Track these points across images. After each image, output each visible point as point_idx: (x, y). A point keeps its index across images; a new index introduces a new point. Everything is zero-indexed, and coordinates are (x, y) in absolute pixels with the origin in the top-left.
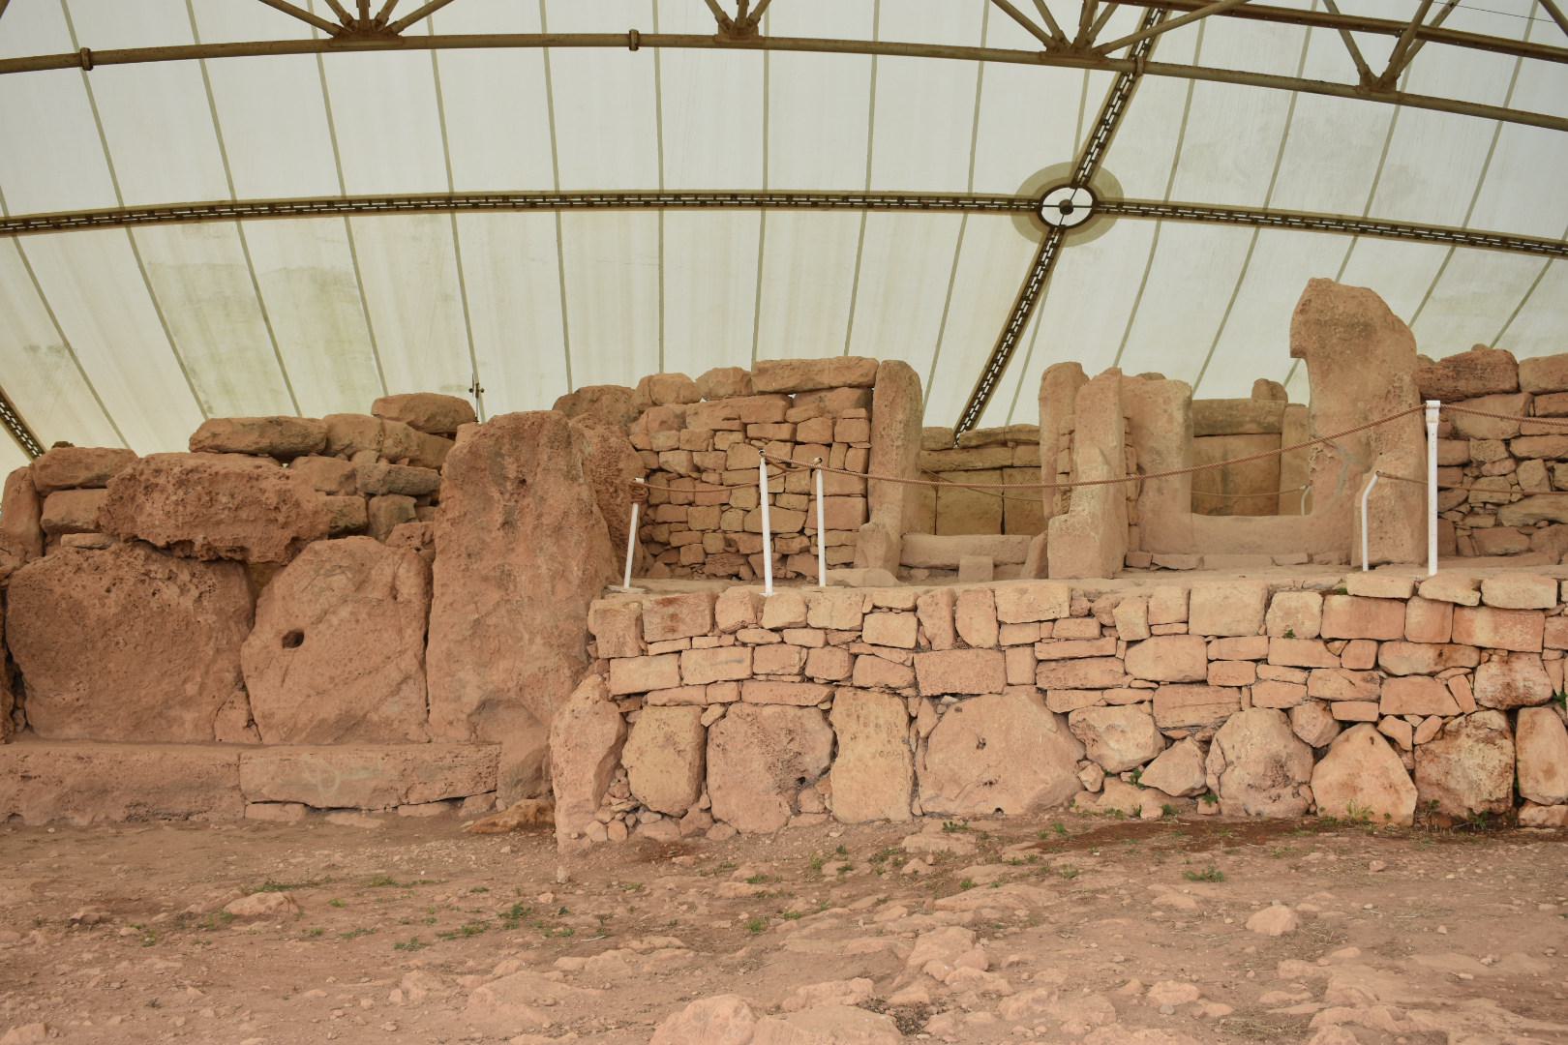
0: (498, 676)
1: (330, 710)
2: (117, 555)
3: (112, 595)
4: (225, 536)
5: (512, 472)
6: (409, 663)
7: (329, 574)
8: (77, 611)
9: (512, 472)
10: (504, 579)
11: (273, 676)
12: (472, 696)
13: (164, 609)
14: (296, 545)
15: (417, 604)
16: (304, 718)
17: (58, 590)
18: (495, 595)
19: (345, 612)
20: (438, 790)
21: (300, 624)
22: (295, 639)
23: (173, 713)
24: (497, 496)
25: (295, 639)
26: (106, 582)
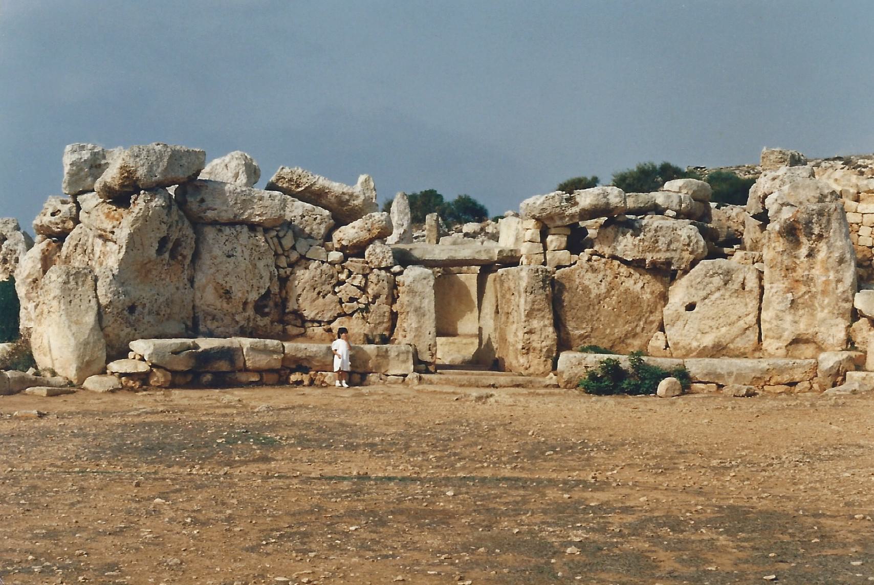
0: (803, 327)
1: (708, 341)
2: (605, 264)
3: (603, 284)
4: (661, 256)
5: (816, 231)
6: (751, 319)
7: (712, 276)
8: (586, 289)
9: (816, 231)
10: (809, 281)
11: (680, 324)
12: (788, 336)
13: (627, 291)
14: (693, 264)
15: (757, 291)
16: (695, 344)
17: (578, 281)
18: (803, 289)
19: (717, 295)
20: (786, 378)
21: (695, 299)
22: (691, 307)
23: (629, 341)
24: (803, 239)
25: (691, 307)
26: (600, 277)
